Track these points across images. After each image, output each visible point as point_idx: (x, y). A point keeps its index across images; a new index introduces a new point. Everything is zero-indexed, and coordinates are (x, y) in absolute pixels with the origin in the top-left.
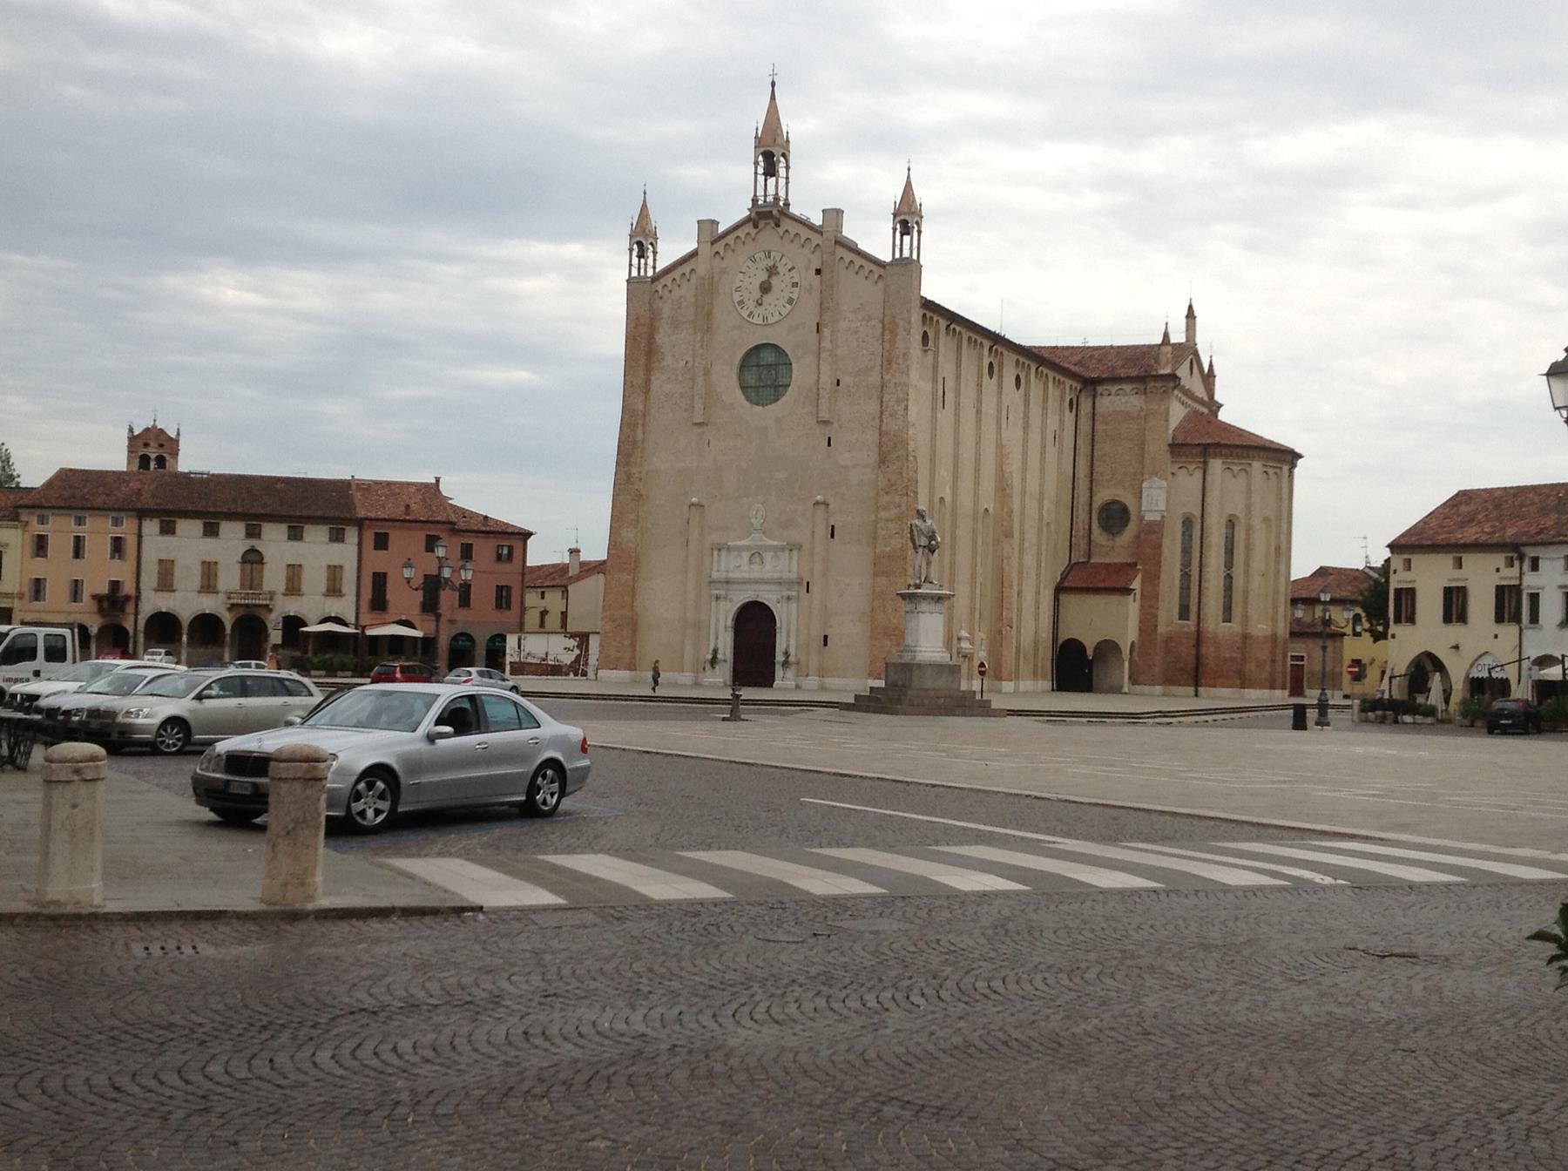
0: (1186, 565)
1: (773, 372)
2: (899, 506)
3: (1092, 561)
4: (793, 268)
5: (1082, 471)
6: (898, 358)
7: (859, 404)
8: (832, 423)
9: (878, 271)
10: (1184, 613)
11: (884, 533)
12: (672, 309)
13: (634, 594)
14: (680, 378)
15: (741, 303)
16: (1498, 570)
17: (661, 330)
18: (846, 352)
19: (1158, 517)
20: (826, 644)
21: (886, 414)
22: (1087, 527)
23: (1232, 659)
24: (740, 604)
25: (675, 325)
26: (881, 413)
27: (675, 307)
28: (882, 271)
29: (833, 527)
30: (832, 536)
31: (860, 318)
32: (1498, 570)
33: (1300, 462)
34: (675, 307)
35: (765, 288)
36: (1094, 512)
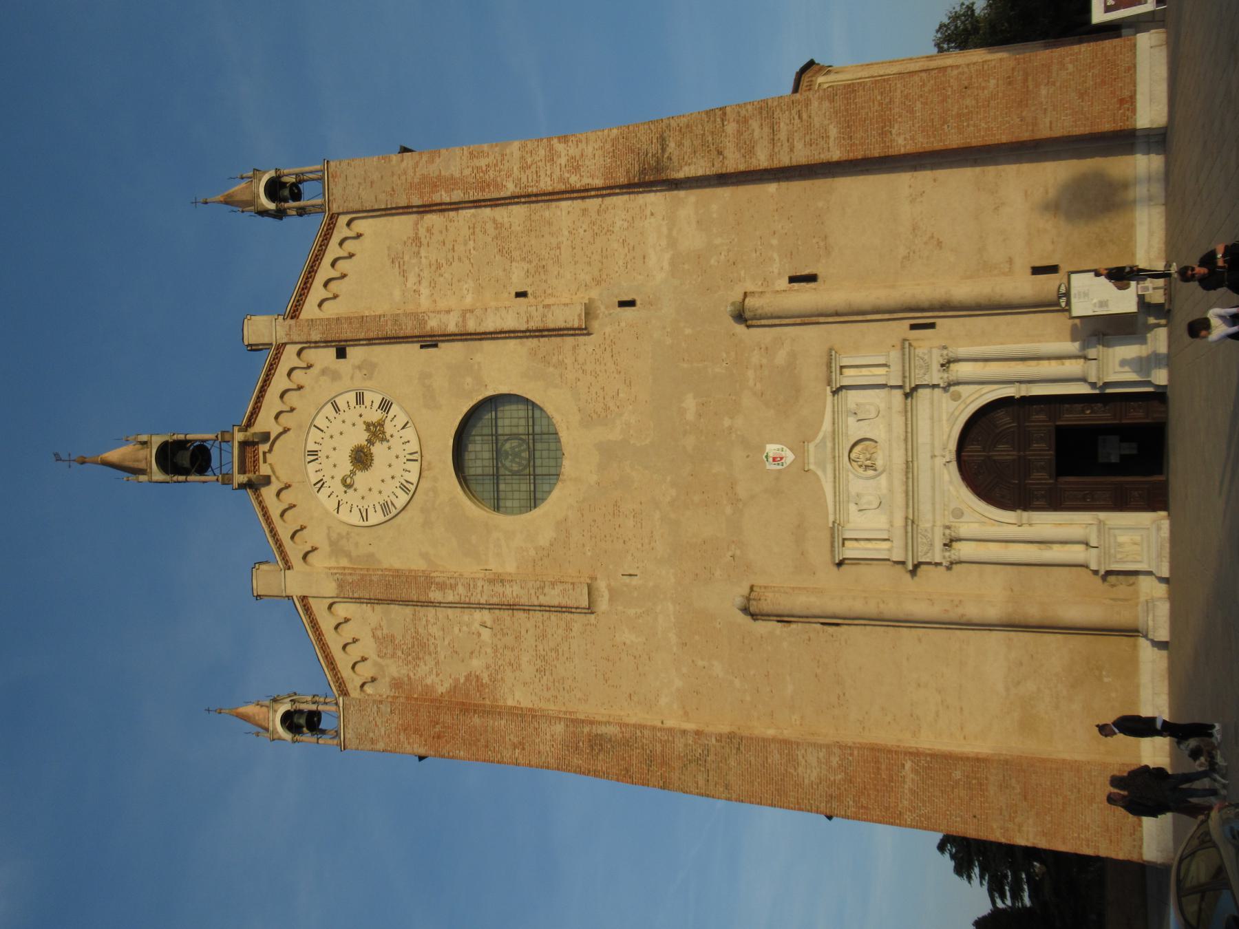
1: (507, 446)
9: (341, 231)
11: (799, 145)
12: (393, 656)
17: (429, 681)
18: (470, 284)
21: (575, 181)
25: (418, 648)
28: (343, 220)
29: (793, 279)
30: (812, 278)
31: (414, 261)
35: (361, 458)
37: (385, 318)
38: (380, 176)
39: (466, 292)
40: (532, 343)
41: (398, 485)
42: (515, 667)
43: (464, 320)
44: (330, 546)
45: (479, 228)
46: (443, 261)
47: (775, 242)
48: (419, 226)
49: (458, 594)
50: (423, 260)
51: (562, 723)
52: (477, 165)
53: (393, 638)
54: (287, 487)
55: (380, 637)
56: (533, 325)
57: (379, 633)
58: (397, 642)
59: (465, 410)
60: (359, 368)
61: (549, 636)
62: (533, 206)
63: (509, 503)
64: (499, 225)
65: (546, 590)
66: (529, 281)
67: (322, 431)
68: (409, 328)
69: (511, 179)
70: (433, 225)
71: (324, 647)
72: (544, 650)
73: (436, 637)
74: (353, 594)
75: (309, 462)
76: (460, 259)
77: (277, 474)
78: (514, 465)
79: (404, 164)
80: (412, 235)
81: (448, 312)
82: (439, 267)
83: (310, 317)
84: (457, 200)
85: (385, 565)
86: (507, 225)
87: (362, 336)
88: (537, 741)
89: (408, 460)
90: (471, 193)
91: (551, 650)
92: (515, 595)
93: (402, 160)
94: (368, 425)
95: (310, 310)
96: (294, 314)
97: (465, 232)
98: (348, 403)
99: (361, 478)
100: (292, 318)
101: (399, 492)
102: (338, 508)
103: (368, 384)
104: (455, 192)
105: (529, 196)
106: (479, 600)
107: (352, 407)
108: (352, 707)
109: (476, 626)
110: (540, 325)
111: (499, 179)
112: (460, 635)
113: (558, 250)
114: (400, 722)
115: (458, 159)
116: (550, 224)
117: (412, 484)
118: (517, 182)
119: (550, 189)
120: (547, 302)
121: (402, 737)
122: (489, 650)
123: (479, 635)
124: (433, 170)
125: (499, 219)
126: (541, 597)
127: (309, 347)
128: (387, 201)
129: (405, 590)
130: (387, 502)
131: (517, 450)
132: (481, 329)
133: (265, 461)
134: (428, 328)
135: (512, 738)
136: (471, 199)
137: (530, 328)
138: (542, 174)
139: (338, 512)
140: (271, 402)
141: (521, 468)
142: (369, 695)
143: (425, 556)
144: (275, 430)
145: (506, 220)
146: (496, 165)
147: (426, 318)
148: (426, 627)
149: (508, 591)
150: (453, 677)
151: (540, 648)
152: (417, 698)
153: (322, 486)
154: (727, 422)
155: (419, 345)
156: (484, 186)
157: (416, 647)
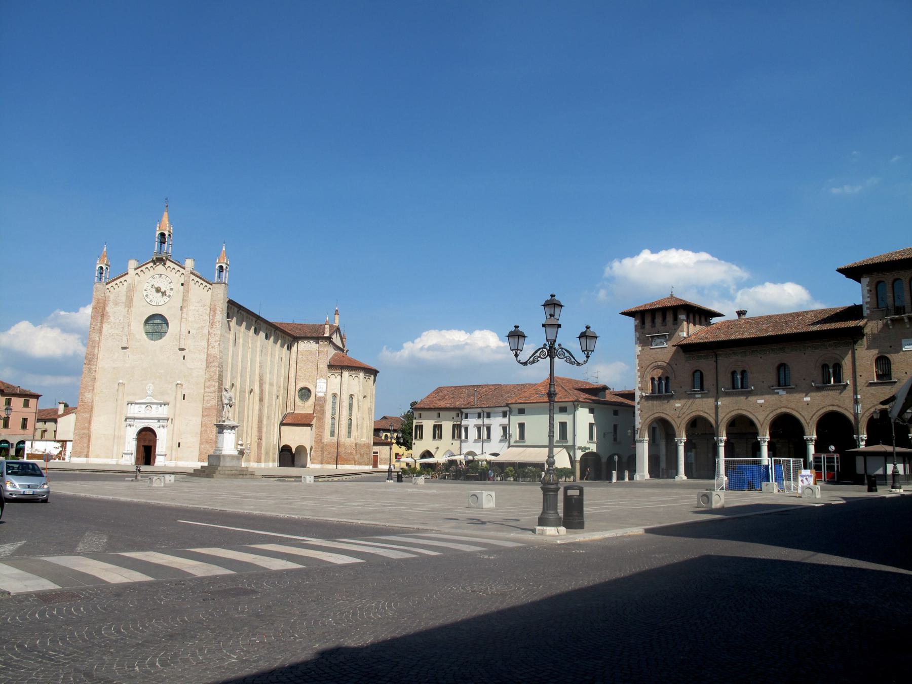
0: (334, 414)
2: (214, 386)
3: (295, 412)
4: (171, 282)
5: (292, 375)
6: (216, 323)
8: (185, 349)
9: (209, 286)
10: (332, 434)
11: (207, 398)
13: (90, 423)
14: (117, 327)
15: (147, 296)
16: (453, 418)
18: (193, 319)
19: (322, 394)
20: (179, 446)
22: (294, 398)
23: (351, 453)
24: (140, 429)
25: (116, 304)
26: (208, 346)
27: (117, 296)
28: (210, 286)
29: (184, 395)
30: (184, 399)
32: (453, 418)
33: (378, 374)
34: (117, 296)
35: (158, 290)
36: (296, 392)
47: (192, 391)
59: (166, 317)
71: (117, 279)
81: (187, 314)
94: (165, 292)
95: (192, 277)
97: (205, 318)
99: (154, 290)
109: (120, 318)
116: (203, 340)
134: (184, 309)
140: (172, 265)
144: (166, 266)
148: (121, 305)
154: (158, 379)
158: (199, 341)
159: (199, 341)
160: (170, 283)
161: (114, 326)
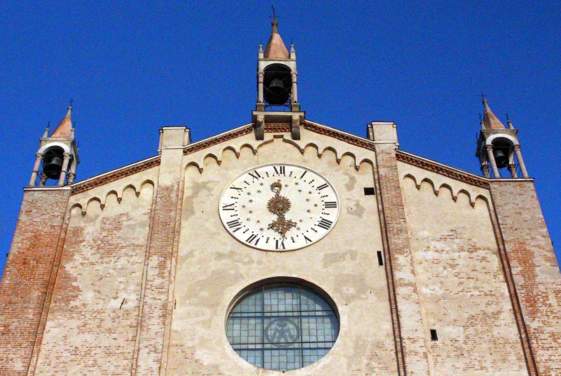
7: (482, 368)
9: (475, 191)
12: (102, 229)
14: (108, 324)
17: (77, 257)
18: (440, 292)
28: (484, 192)
31: (455, 247)
37: (402, 223)
38: (526, 219)
39: (432, 288)
40: (389, 344)
41: (255, 234)
42: (82, 328)
43: (406, 285)
44: (203, 183)
45: (491, 300)
46: (457, 270)
48: (487, 251)
49: (154, 279)
50: (456, 255)
51: (23, 369)
52: (550, 297)
53: (118, 228)
54: (255, 152)
55: (120, 219)
56: (407, 343)
57: (124, 218)
58: (114, 232)
59: (324, 287)
60: (357, 205)
61: (109, 359)
62: (519, 346)
63: (237, 327)
64: (496, 316)
65: (153, 355)
66: (448, 342)
67: (302, 177)
68: (396, 241)
69: (541, 325)
70: (489, 262)
72: (95, 354)
73: (116, 263)
74: (159, 197)
75: (275, 168)
76: (461, 283)
77: (264, 146)
78: (273, 332)
79: (539, 237)
80: (478, 245)
81: (413, 272)
82: (453, 266)
83: (398, 167)
84: (514, 280)
85: (184, 223)
86: (497, 323)
87: (386, 205)
88: (9, 346)
89: (277, 241)
90: (523, 291)
91: (95, 361)
92: (150, 327)
93: (543, 236)
95: (404, 168)
96: (399, 157)
98: (327, 196)
100: (397, 155)
101: (249, 234)
102: (235, 188)
103: (344, 211)
104: (522, 278)
105: (528, 341)
106: (147, 296)
107: (323, 199)
108: (61, 196)
109: (123, 295)
110: (407, 350)
111: (539, 314)
112: (117, 283)
113: (479, 368)
114: (43, 233)
115: (552, 281)
116: (504, 360)
117: (256, 244)
118: (539, 330)
119: (538, 359)
120: (430, 357)
121: (30, 234)
122: (100, 307)
123: (116, 298)
124: (538, 260)
125: (502, 316)
126: (147, 350)
127: (373, 168)
128: (506, 224)
129: (160, 236)
130: (240, 225)
131: (287, 334)
132: (399, 299)
133: (275, 137)
134: (397, 256)
135: (14, 324)
136: (518, 291)
137: (404, 341)
138: (551, 352)
139: (231, 188)
140: (323, 141)
141: (270, 338)
142: (70, 210)
143: (191, 254)
144: (302, 143)
145: (502, 322)
146: (552, 312)
147: (405, 255)
148: (127, 255)
149: (155, 321)
150: (78, 276)
151: (98, 351)
152: (63, 247)
153: (254, 176)
155: (381, 249)
156: (532, 301)
157: (109, 247)
158: (488, 364)
159: (488, 364)
160: (320, 188)
161: (93, 324)
